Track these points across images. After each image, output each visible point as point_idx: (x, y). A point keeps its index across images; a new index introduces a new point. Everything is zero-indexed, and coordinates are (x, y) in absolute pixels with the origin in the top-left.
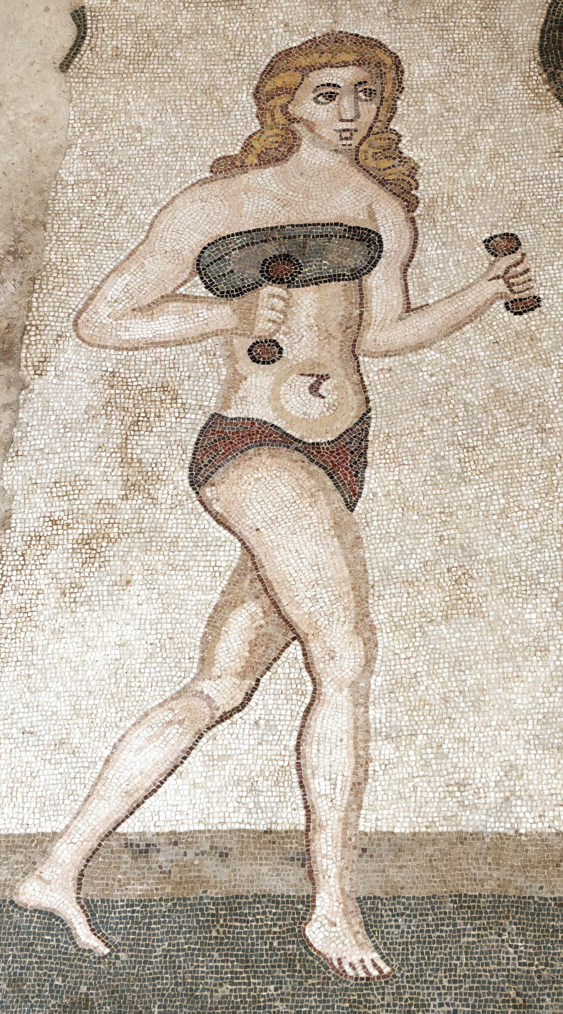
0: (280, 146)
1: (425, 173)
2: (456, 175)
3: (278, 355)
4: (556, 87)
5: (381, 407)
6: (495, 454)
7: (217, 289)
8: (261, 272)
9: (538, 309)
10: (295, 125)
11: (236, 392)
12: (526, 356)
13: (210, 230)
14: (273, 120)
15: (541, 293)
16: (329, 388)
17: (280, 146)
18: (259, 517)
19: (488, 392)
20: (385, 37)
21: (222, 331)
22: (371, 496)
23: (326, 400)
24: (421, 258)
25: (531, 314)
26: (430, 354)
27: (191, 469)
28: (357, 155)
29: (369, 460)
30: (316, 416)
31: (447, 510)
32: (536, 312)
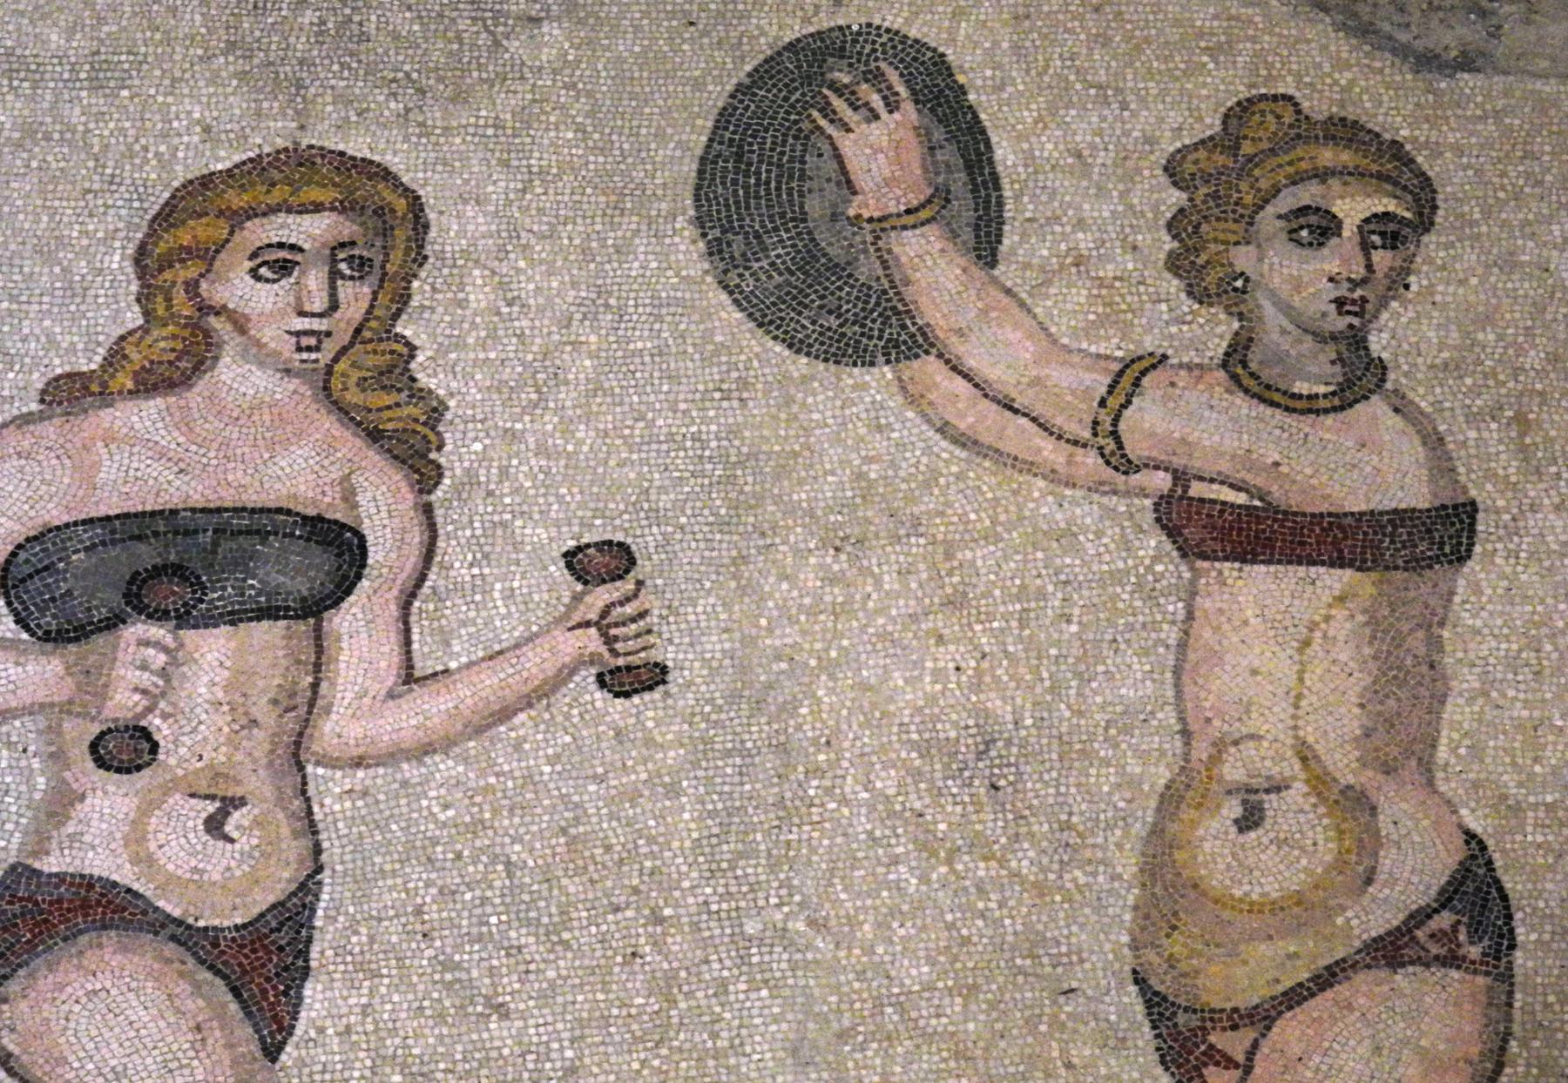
0: (178, 359)
1: (457, 420)
2: (518, 426)
3: (147, 757)
4: (722, 266)
5: (342, 863)
6: (562, 963)
7: (38, 626)
8: (125, 596)
9: (661, 688)
10: (212, 319)
11: (61, 824)
12: (633, 777)
13: (32, 513)
14: (169, 308)
15: (669, 656)
17: (178, 359)
18: (90, 1066)
19: (554, 841)
20: (396, 160)
21: (42, 706)
22: (313, 1034)
23: (237, 846)
24: (441, 582)
25: (647, 696)
26: (445, 767)
28: (326, 381)
29: (313, 964)
30: (216, 877)
31: (459, 1067)
32: (657, 694)
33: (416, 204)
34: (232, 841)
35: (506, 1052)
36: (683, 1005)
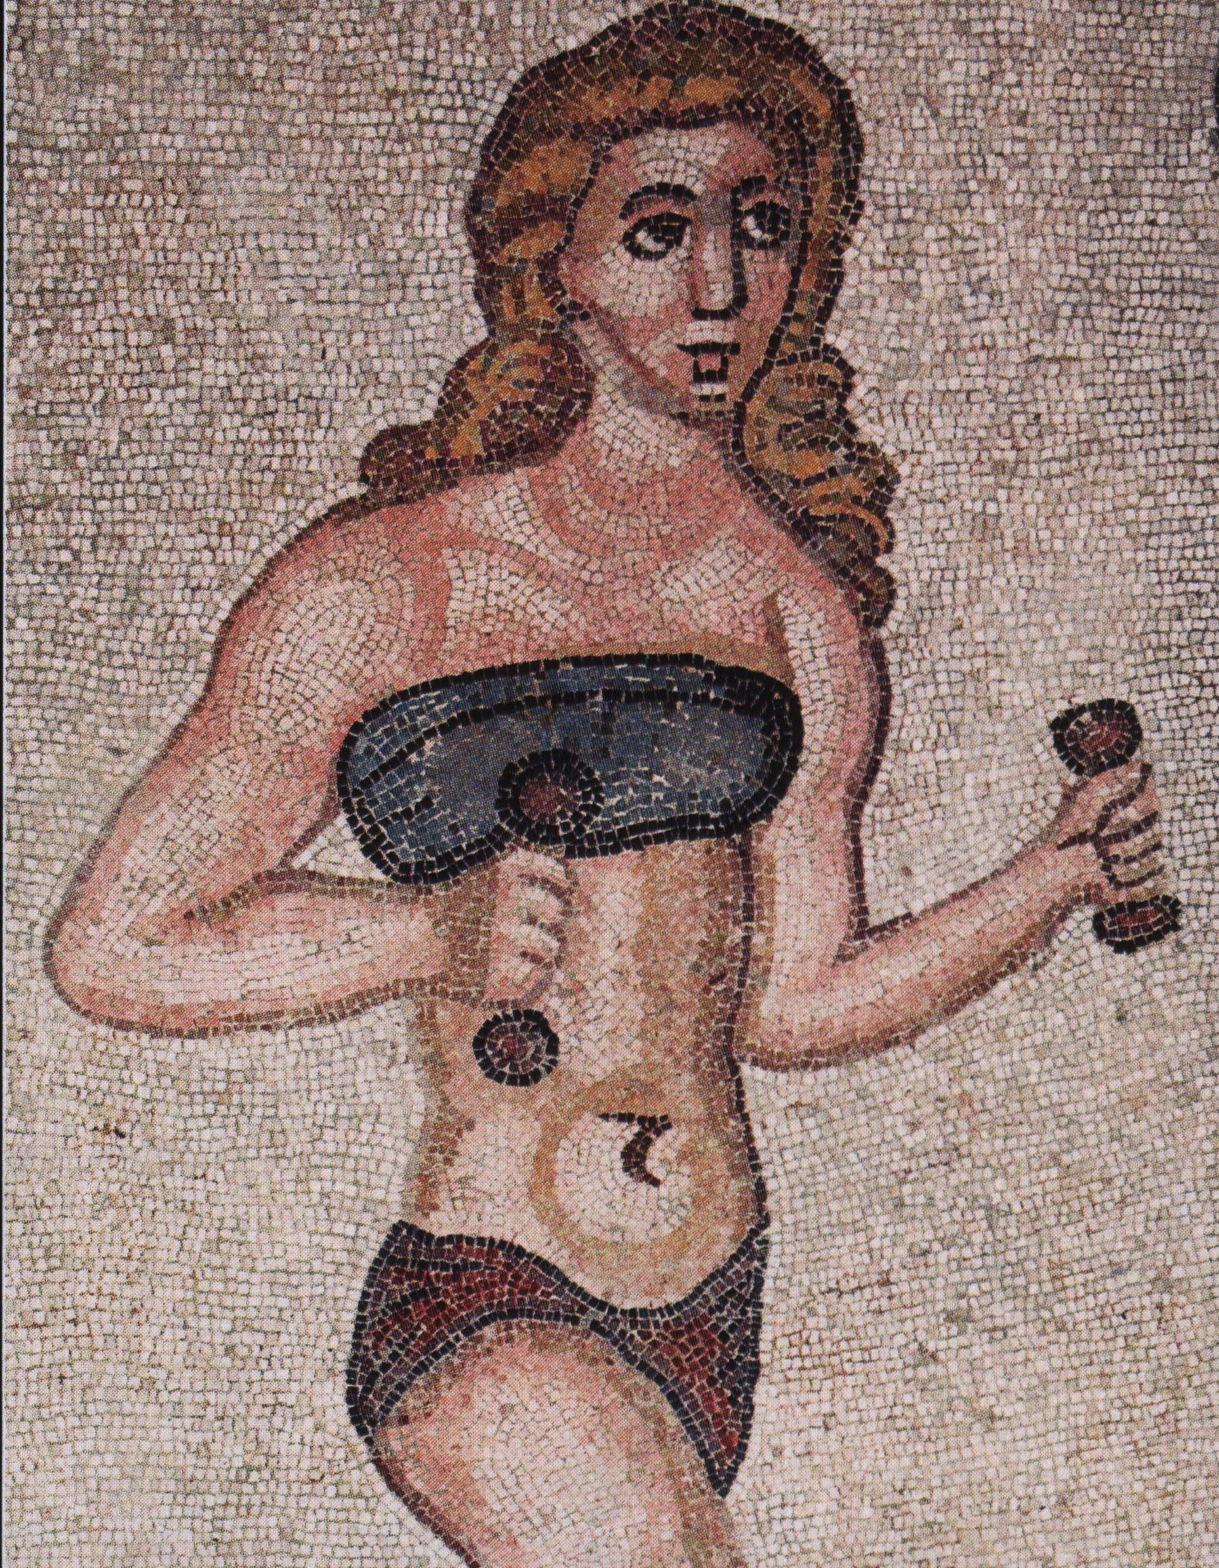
0: (538, 398)
1: (912, 500)
5: (793, 1211)
7: (393, 857)
8: (499, 804)
9: (1171, 936)
10: (579, 327)
13: (368, 672)
16: (671, 1155)
17: (538, 398)
19: (1043, 1176)
22: (769, 1457)
23: (663, 1190)
24: (897, 775)
25: (1154, 950)
27: (350, 1374)
28: (738, 433)
29: (764, 1358)
30: (641, 1238)
31: (937, 1495)
33: (844, 111)
34: (656, 1182)
35: (991, 1473)
36: (1192, 1403)
